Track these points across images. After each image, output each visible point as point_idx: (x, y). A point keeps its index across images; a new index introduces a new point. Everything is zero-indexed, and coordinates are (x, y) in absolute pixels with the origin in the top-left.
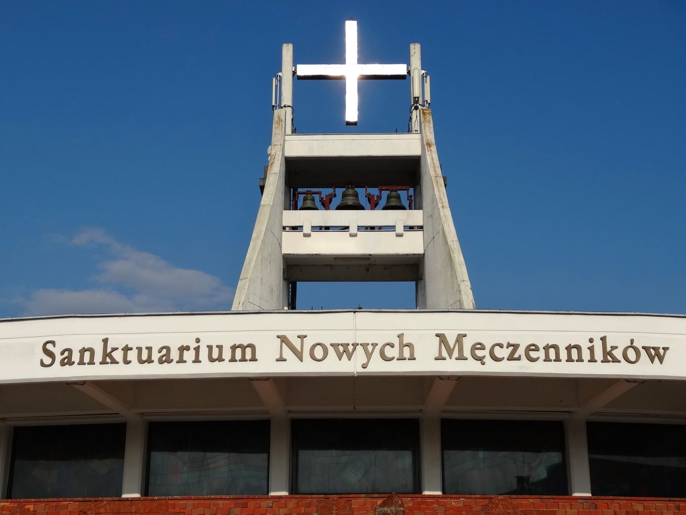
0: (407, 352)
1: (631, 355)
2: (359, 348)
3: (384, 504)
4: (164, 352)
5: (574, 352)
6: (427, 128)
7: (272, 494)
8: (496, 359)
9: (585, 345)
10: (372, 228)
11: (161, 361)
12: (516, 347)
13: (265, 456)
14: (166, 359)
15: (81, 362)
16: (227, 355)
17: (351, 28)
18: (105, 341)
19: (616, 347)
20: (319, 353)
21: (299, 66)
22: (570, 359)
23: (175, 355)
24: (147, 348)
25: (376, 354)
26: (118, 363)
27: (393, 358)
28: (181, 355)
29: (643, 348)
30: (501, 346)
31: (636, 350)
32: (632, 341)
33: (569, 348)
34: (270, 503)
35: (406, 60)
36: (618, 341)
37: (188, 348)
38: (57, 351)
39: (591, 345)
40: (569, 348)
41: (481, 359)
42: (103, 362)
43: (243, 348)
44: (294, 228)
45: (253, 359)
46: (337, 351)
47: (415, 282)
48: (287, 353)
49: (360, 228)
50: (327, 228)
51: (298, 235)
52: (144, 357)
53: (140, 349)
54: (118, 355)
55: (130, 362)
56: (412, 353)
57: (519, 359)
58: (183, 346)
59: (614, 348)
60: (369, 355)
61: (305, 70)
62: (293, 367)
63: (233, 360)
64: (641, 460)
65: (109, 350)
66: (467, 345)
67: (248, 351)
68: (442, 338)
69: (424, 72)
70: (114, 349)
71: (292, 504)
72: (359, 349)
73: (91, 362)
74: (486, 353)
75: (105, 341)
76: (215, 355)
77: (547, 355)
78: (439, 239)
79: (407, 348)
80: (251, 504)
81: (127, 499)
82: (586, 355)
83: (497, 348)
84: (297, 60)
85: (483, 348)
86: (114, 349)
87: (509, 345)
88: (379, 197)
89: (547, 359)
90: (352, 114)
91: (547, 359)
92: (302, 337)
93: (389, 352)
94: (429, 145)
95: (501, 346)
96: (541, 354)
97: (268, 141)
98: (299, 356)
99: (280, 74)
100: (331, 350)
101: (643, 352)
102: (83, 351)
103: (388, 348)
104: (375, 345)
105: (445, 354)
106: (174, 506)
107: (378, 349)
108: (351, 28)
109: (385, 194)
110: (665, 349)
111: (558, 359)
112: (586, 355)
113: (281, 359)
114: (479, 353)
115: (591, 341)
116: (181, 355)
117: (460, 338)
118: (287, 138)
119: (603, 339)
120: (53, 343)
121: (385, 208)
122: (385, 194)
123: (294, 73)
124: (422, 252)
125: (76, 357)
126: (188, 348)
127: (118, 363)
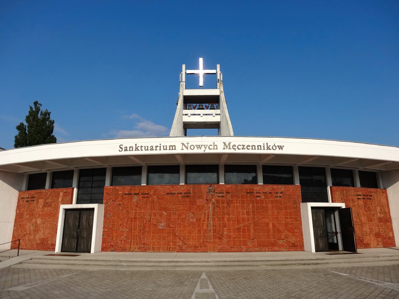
0: (215, 147)
1: (274, 148)
2: (203, 146)
3: (209, 187)
4: (152, 147)
5: (259, 147)
6: (221, 88)
7: (180, 184)
8: (239, 149)
9: (262, 145)
11: (151, 150)
12: (244, 146)
13: (178, 174)
14: (152, 149)
15: (130, 150)
16: (168, 148)
17: (201, 60)
18: (136, 145)
19: (270, 146)
20: (192, 147)
21: (187, 70)
22: (258, 149)
23: (154, 148)
24: (147, 146)
26: (139, 150)
27: (212, 149)
28: (156, 148)
29: (277, 146)
30: (240, 145)
31: (275, 146)
32: (274, 144)
33: (258, 146)
34: (180, 186)
35: (215, 68)
36: (271, 144)
37: (158, 146)
38: (123, 147)
39: (264, 145)
40: (258, 146)
41: (235, 149)
42: (135, 150)
43: (172, 146)
44: (186, 115)
45: (175, 149)
46: (197, 147)
48: (184, 148)
49: (203, 115)
50: (195, 115)
51: (187, 116)
52: (146, 149)
53: (145, 147)
54: (139, 148)
55: (142, 150)
56: (217, 147)
57: (245, 149)
58: (16, 137)
59: (270, 146)
60: (205, 148)
61: (189, 71)
62: (185, 151)
63: (170, 149)
64: (276, 175)
65: (137, 147)
66: (231, 145)
67: (174, 147)
68: (225, 143)
69: (220, 72)
70: (138, 147)
71: (185, 187)
73: (132, 150)
74: (236, 147)
75: (136, 145)
76: (165, 148)
77: (252, 148)
78: (224, 117)
79: (215, 146)
80: (175, 187)
81: (143, 186)
82: (262, 148)
83: (239, 146)
84: (187, 68)
85: (235, 146)
86: (138, 147)
87: (242, 145)
88: (209, 106)
89: (252, 149)
90: (201, 83)
91: (252, 149)
92: (188, 143)
93: (211, 147)
94: (222, 92)
95: (240, 145)
96: (251, 148)
97: (179, 91)
99: (182, 73)
100: (195, 147)
101: (277, 147)
102: (130, 147)
103: (210, 146)
104: (207, 145)
105: (225, 148)
106: (155, 187)
107: (208, 146)
108: (201, 60)
109: (210, 105)
110: (283, 146)
111: (255, 149)
112: (262, 148)
113: (182, 149)
114: (234, 147)
115: (264, 144)
116: (156, 148)
117: (229, 143)
118: (184, 90)
119: (267, 144)
120: (122, 145)
121: (210, 109)
122: (210, 105)
123: (186, 72)
124: (220, 121)
125: (128, 149)
126: (158, 146)
127: (139, 150)
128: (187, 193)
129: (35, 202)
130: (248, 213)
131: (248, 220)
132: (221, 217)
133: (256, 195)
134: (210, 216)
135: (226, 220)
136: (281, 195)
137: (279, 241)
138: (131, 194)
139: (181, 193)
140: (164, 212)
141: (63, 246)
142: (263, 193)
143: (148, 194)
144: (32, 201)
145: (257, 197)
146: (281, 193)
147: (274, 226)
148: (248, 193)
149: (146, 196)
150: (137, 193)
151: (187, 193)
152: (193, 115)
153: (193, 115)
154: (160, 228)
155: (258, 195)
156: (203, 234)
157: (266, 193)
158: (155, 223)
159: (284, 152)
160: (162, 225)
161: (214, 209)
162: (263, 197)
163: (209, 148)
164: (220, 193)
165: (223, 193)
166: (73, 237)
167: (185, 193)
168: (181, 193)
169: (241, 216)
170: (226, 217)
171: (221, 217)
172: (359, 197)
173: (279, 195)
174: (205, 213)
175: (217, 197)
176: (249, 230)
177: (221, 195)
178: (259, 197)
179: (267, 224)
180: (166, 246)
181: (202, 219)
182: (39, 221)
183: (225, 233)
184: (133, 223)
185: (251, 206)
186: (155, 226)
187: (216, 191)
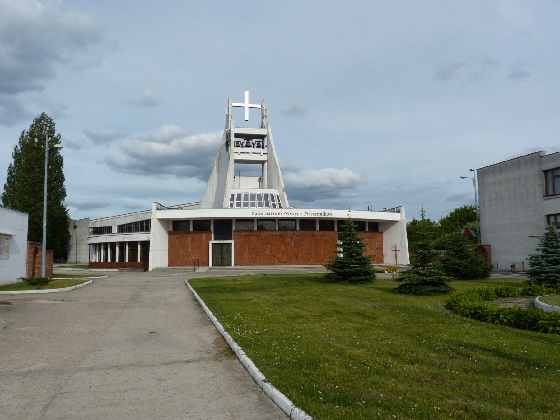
1: (328, 215)
10: (255, 153)
12: (314, 214)
16: (278, 214)
17: (247, 93)
20: (290, 214)
23: (271, 214)
25: (297, 214)
36: (326, 213)
38: (254, 213)
41: (310, 215)
47: (261, 165)
48: (286, 214)
50: (243, 153)
54: (263, 214)
60: (296, 214)
66: (308, 213)
68: (305, 212)
72: (295, 214)
79: (301, 214)
82: (322, 215)
85: (310, 214)
96: (317, 214)
98: (287, 214)
108: (247, 93)
112: (322, 215)
117: (307, 213)
123: (232, 105)
125: (257, 214)
128: (281, 235)
129: (184, 238)
131: (311, 249)
132: (298, 247)
133: (316, 236)
134: (293, 247)
135: (300, 248)
136: (328, 236)
137: (325, 260)
138: (249, 235)
139: (277, 235)
140: (268, 245)
141: (213, 263)
142: (319, 235)
143: (259, 235)
144: (182, 238)
145: (316, 237)
146: (328, 235)
147: (323, 251)
148: (311, 235)
149: (258, 236)
150: (253, 234)
151: (281, 235)
154: (267, 253)
155: (317, 236)
156: (289, 256)
157: (320, 235)
158: (264, 251)
160: (267, 252)
161: (295, 243)
162: (319, 237)
163: (298, 215)
164: (297, 235)
165: (299, 235)
166: (219, 258)
167: (279, 235)
168: (277, 235)
169: (308, 247)
170: (300, 248)
171: (298, 247)
172: (367, 237)
173: (327, 236)
174: (290, 246)
175: (296, 238)
176: (312, 254)
177: (298, 236)
178: (317, 237)
179: (320, 251)
180: (270, 262)
181: (288, 248)
182: (190, 250)
183: (300, 256)
184: (252, 251)
185: (313, 242)
186: (264, 252)
187: (296, 234)
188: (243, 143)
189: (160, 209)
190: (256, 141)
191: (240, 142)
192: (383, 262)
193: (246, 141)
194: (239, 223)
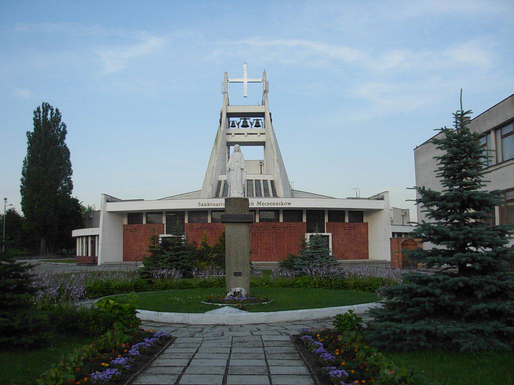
10: (251, 134)
14: (217, 205)
117: (260, 202)
130: (273, 240)
131: (273, 243)
152: (237, 134)
153: (237, 134)
159: (292, 206)
176: (273, 249)
183: (259, 251)
188: (239, 123)
189: (112, 202)
190: (254, 120)
191: (235, 122)
192: (368, 258)
193: (242, 121)
194: (261, 212)
